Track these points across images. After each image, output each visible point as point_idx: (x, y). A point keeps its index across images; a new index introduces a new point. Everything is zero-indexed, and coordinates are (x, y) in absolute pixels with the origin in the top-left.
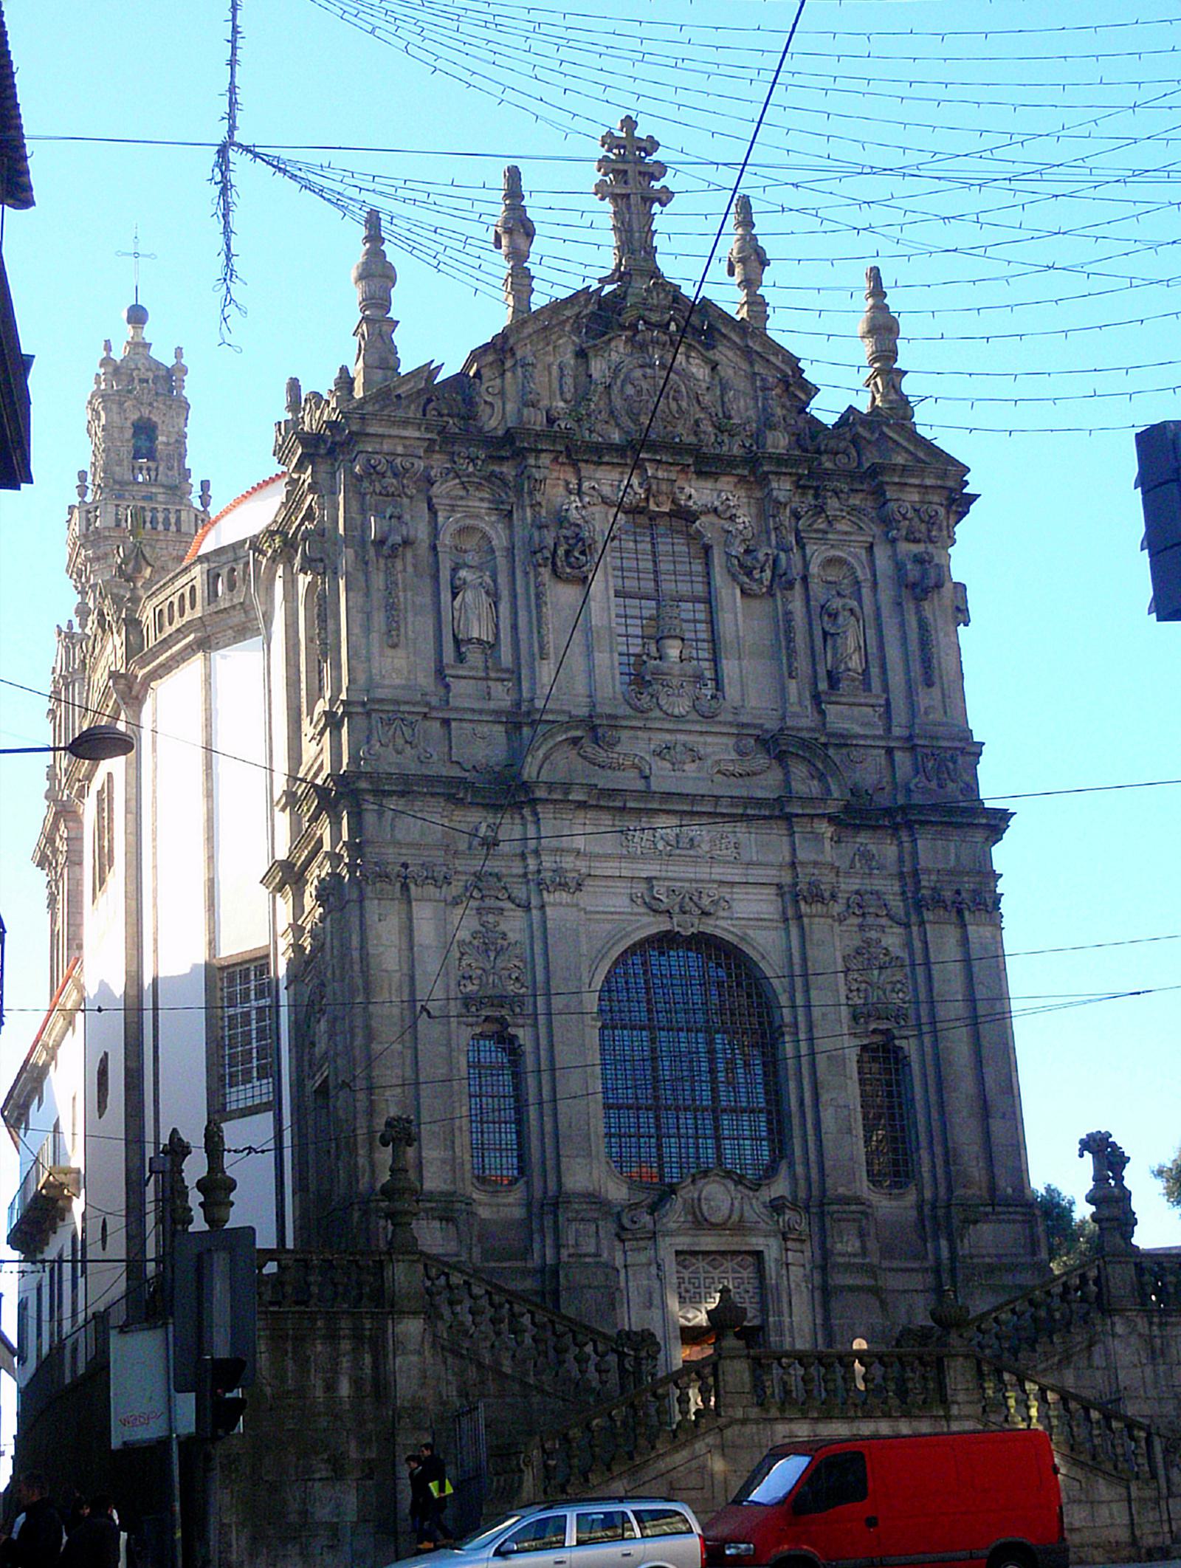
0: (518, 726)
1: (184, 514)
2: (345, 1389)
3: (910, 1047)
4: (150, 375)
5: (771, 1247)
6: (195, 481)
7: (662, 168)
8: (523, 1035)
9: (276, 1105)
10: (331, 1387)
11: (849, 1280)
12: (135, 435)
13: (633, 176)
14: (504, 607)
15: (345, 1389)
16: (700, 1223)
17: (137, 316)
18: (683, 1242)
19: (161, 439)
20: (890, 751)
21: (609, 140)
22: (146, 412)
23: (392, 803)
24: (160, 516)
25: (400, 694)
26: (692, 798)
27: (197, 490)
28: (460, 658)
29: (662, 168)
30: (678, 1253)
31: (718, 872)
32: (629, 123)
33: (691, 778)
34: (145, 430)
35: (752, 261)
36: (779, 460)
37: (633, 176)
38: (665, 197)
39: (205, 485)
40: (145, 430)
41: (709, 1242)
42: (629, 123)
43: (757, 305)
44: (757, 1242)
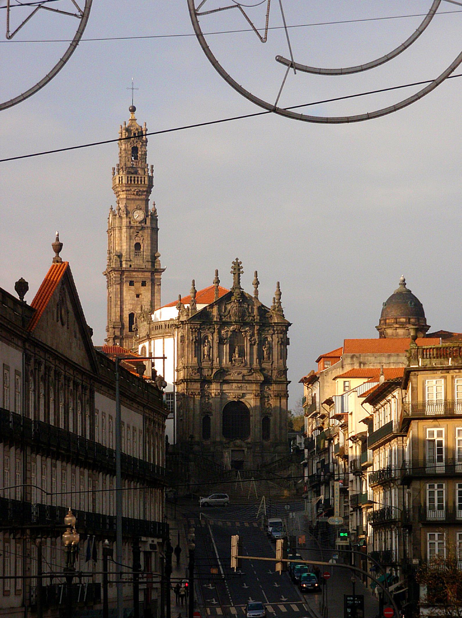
0: (212, 369)
1: (146, 179)
2: (183, 471)
3: (271, 418)
4: (137, 132)
5: (246, 450)
6: (149, 167)
7: (242, 267)
8: (211, 417)
9: (174, 418)
10: (182, 470)
11: (257, 454)
12: (132, 152)
13: (237, 269)
14: (211, 349)
15: (183, 471)
16: (235, 446)
17: (133, 110)
18: (232, 449)
19: (140, 153)
20: (272, 370)
21: (233, 263)
22: (135, 145)
23: (193, 383)
24: (139, 179)
25: (195, 365)
26: (239, 380)
27: (149, 167)
28: (204, 357)
29: (242, 267)
30: (232, 451)
31: (243, 392)
32: (237, 259)
33: (240, 377)
34: (135, 150)
35: (257, 283)
36: (257, 323)
37: (237, 269)
38: (243, 272)
39: (152, 166)
40: (135, 150)
41: (237, 449)
42: (237, 259)
43: (256, 292)
44: (244, 449)
